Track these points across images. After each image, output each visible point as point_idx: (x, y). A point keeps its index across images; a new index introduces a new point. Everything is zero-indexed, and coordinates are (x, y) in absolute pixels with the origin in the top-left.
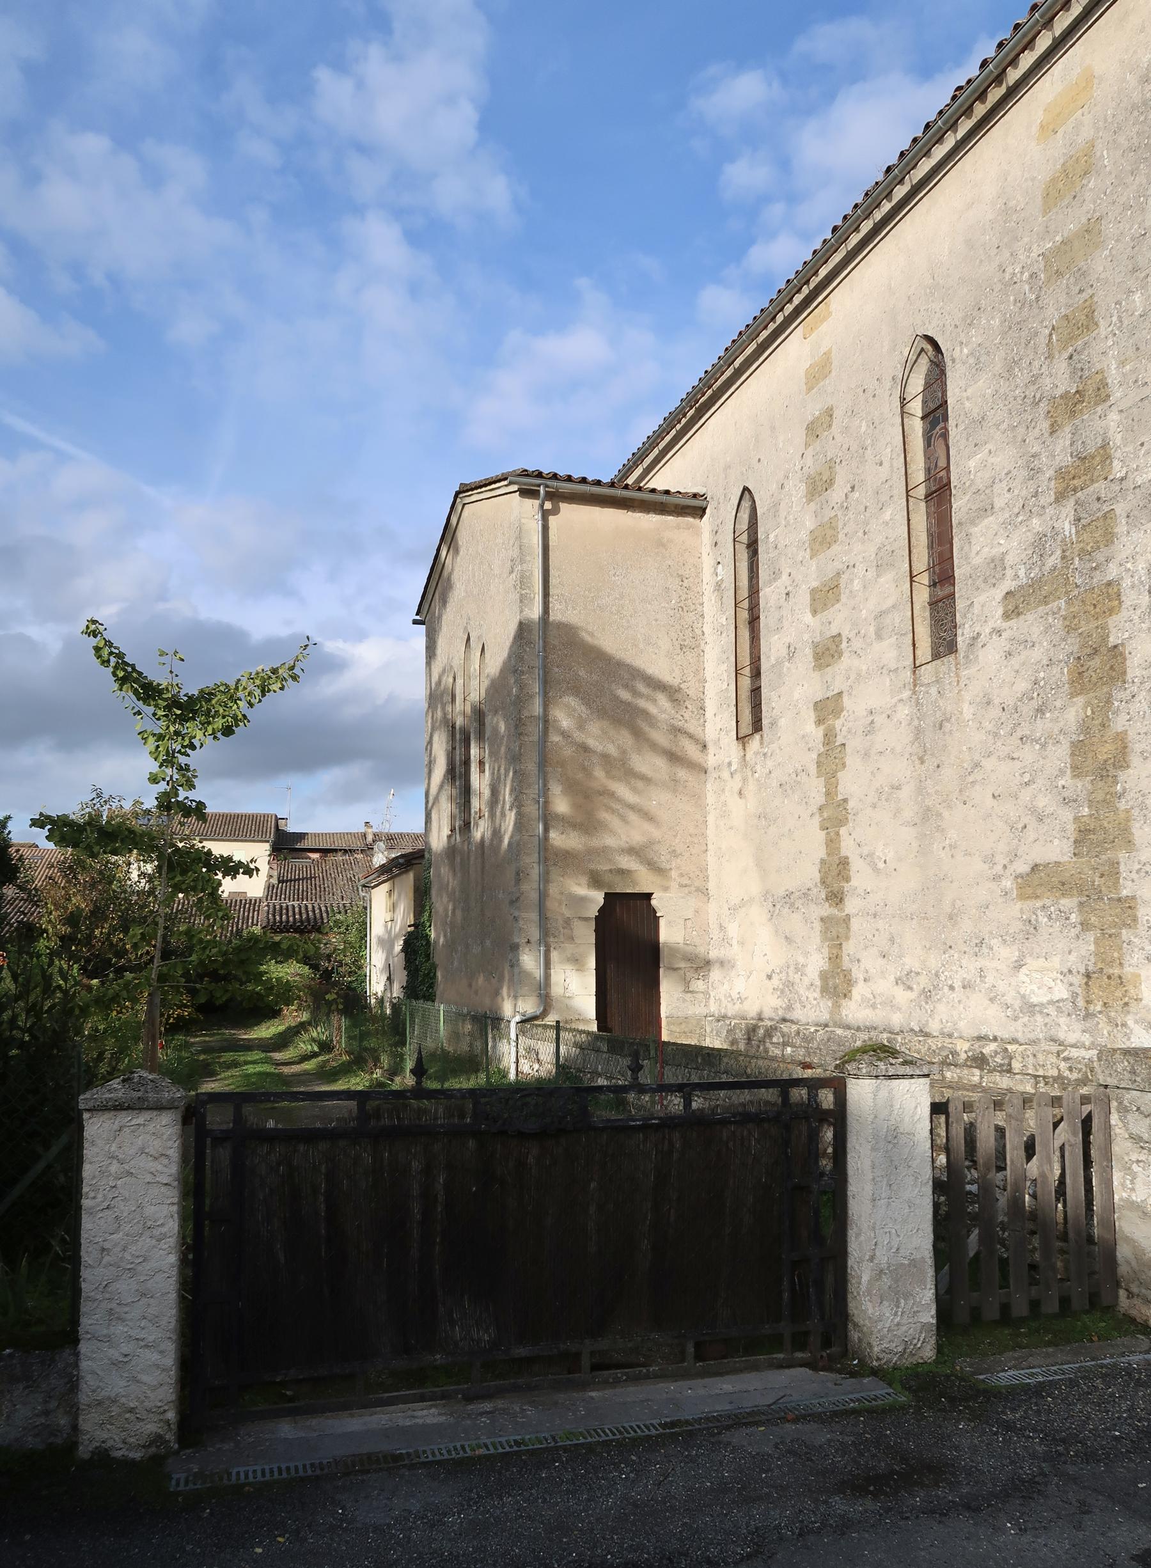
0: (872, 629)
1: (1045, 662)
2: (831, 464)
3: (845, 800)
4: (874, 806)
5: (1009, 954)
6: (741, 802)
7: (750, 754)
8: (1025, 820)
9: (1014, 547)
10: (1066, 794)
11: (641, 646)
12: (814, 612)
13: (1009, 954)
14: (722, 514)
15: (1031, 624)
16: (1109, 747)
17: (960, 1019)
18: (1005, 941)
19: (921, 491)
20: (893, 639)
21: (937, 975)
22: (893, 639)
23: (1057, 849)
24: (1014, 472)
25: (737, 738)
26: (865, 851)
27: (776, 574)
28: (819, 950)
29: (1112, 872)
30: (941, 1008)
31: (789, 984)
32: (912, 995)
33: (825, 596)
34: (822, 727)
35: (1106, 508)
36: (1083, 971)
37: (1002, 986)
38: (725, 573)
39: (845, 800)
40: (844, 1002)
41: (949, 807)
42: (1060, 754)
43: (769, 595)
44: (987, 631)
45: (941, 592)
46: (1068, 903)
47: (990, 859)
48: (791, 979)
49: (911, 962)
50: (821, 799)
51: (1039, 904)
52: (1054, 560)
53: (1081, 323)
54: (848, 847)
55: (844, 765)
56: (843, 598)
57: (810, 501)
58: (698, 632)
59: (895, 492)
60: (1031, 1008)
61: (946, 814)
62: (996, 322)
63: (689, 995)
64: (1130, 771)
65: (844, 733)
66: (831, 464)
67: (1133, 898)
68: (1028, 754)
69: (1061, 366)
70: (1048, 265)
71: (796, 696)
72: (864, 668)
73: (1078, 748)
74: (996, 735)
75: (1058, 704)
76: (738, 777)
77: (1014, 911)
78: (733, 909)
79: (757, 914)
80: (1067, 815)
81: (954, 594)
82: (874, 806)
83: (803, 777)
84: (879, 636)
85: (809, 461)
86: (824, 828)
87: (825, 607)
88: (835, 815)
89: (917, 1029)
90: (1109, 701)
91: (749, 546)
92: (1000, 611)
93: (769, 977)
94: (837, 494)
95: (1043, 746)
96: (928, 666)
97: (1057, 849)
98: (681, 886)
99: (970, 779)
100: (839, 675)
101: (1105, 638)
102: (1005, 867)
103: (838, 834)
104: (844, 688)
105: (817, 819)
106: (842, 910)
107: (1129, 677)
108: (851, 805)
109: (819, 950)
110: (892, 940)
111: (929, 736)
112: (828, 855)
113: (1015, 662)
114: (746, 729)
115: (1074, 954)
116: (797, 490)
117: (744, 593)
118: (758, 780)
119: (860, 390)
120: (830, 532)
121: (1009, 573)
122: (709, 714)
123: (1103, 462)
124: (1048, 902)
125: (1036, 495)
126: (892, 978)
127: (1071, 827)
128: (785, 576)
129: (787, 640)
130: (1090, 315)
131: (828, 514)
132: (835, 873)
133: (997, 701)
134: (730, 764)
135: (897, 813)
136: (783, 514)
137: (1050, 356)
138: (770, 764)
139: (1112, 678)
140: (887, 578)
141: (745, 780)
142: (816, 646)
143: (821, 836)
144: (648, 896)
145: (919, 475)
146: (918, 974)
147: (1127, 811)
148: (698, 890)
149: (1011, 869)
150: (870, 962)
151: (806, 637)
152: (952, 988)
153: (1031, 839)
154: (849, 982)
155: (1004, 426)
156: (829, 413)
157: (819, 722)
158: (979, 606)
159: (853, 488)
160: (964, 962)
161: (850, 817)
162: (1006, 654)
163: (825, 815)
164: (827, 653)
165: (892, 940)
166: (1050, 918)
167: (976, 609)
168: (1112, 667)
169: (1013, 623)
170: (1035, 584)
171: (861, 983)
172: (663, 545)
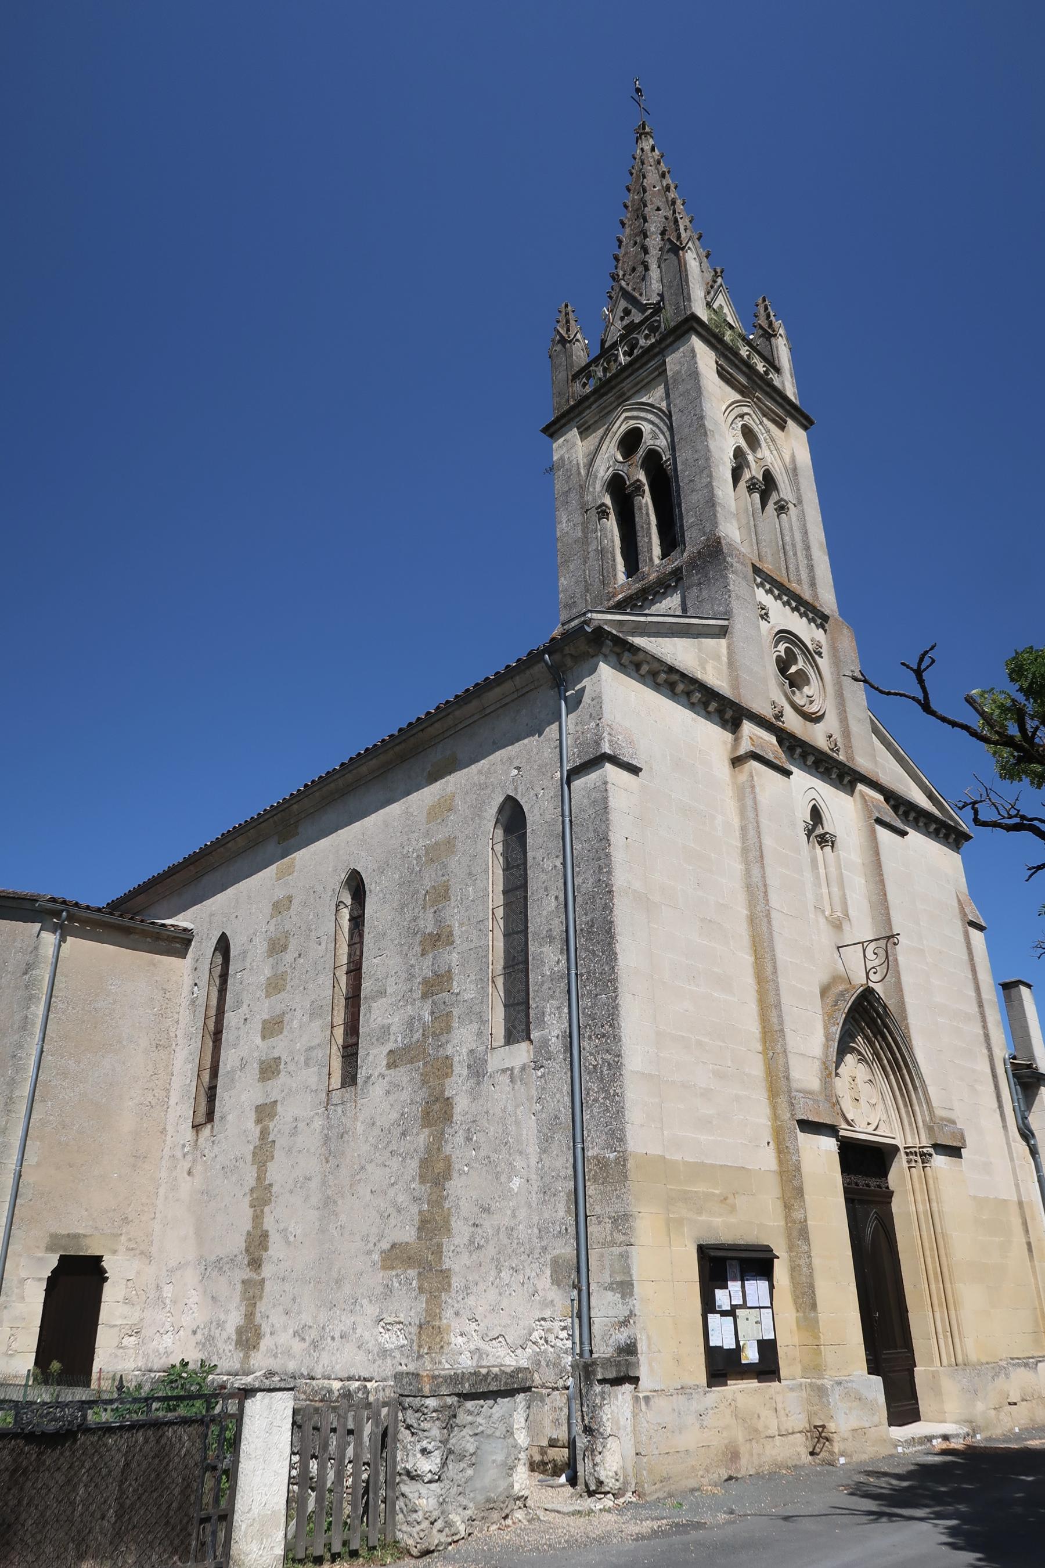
0: (302, 1059)
1: (409, 1101)
2: (287, 934)
3: (271, 1185)
4: (291, 1192)
5: (371, 1310)
6: (188, 1178)
7: (201, 1140)
8: (390, 1210)
9: (396, 1022)
10: (416, 1194)
11: (124, 1043)
12: (264, 1038)
13: (371, 1310)
14: (203, 948)
15: (402, 1075)
16: (441, 1164)
17: (337, 1363)
18: (371, 1301)
19: (345, 968)
20: (316, 1069)
21: (323, 1328)
22: (316, 1069)
23: (408, 1234)
24: (400, 973)
25: (193, 1127)
26: (282, 1226)
27: (239, 1004)
28: (237, 1308)
29: (438, 1251)
30: (325, 1355)
31: (210, 1339)
33: (272, 1027)
34: (260, 1126)
35: (448, 1009)
36: (418, 1323)
37: (367, 1335)
38: (201, 993)
39: (271, 1185)
40: (252, 1354)
41: (343, 1196)
42: (414, 1165)
43: (231, 1018)
44: (377, 1074)
45: (351, 1041)
46: (412, 1273)
47: (366, 1239)
48: (212, 1333)
49: (306, 1318)
50: (252, 1183)
51: (394, 1273)
52: (417, 1036)
53: (441, 895)
54: (269, 1223)
55: (273, 1157)
56: (285, 1033)
57: (269, 956)
58: (172, 1035)
59: (327, 966)
60: (384, 1353)
61: (340, 1202)
62: (396, 876)
63: (121, 1350)
64: (452, 1182)
65: (275, 1132)
66: (287, 934)
67: (450, 1270)
68: (395, 1163)
69: (429, 915)
70: (427, 853)
71: (243, 1098)
72: (294, 1085)
73: (424, 1163)
74: (376, 1147)
75: (415, 1131)
76: (189, 1157)
77: (376, 1279)
78: (171, 1271)
79: (191, 1276)
80: (415, 1210)
81: (357, 1044)
82: (291, 1192)
83: (241, 1164)
84: (307, 1064)
85: (272, 928)
86: (252, 1206)
87: (272, 1035)
88: (261, 1196)
89: (305, 1373)
90: (443, 1134)
91: (220, 976)
92: (385, 1063)
93: (194, 1333)
94: (289, 956)
95: (404, 1159)
96: (337, 1092)
97: (408, 1234)
98: (129, 1249)
99: (358, 1177)
100: (275, 1089)
101: (443, 1092)
102: (375, 1244)
103: (262, 1211)
104: (279, 1098)
105: (248, 1199)
106: (259, 1274)
107: (454, 1120)
108: (274, 1189)
109: (237, 1308)
110: (294, 1300)
111: (334, 1141)
112: (253, 1228)
113: (391, 1098)
114: (201, 1118)
115: (413, 1311)
116: (261, 947)
117: (213, 1012)
118: (205, 1162)
119: (311, 891)
120: (281, 982)
121: (392, 1037)
122: (172, 1102)
123: (448, 981)
124: (399, 1271)
125: (411, 991)
126: (291, 1331)
127: (417, 1218)
128: (245, 1006)
129: (242, 1054)
130: (447, 891)
131: (282, 969)
132: (257, 1243)
133: (378, 1124)
134: (184, 1146)
135: (307, 1198)
136: (249, 960)
137: (424, 908)
138: (216, 1149)
139: (445, 1119)
140: (316, 1025)
141: (194, 1161)
142: (262, 1063)
143: (250, 1212)
144: (99, 1258)
145: (344, 959)
146: (310, 1327)
147: (449, 1209)
148: (142, 1253)
149: (379, 1245)
150: (276, 1318)
151: (256, 1054)
152: (333, 1338)
153: (392, 1225)
154: (259, 1336)
155: (396, 942)
156: (290, 899)
157: (258, 1121)
158: (373, 1058)
159: (300, 955)
160: (343, 1318)
161: (273, 1198)
163: (255, 1196)
164: (269, 1069)
165: (294, 1300)
166: (400, 1284)
167: (371, 1058)
168: (445, 1112)
169: (391, 1072)
170: (407, 1049)
171: (268, 1335)
172: (154, 965)
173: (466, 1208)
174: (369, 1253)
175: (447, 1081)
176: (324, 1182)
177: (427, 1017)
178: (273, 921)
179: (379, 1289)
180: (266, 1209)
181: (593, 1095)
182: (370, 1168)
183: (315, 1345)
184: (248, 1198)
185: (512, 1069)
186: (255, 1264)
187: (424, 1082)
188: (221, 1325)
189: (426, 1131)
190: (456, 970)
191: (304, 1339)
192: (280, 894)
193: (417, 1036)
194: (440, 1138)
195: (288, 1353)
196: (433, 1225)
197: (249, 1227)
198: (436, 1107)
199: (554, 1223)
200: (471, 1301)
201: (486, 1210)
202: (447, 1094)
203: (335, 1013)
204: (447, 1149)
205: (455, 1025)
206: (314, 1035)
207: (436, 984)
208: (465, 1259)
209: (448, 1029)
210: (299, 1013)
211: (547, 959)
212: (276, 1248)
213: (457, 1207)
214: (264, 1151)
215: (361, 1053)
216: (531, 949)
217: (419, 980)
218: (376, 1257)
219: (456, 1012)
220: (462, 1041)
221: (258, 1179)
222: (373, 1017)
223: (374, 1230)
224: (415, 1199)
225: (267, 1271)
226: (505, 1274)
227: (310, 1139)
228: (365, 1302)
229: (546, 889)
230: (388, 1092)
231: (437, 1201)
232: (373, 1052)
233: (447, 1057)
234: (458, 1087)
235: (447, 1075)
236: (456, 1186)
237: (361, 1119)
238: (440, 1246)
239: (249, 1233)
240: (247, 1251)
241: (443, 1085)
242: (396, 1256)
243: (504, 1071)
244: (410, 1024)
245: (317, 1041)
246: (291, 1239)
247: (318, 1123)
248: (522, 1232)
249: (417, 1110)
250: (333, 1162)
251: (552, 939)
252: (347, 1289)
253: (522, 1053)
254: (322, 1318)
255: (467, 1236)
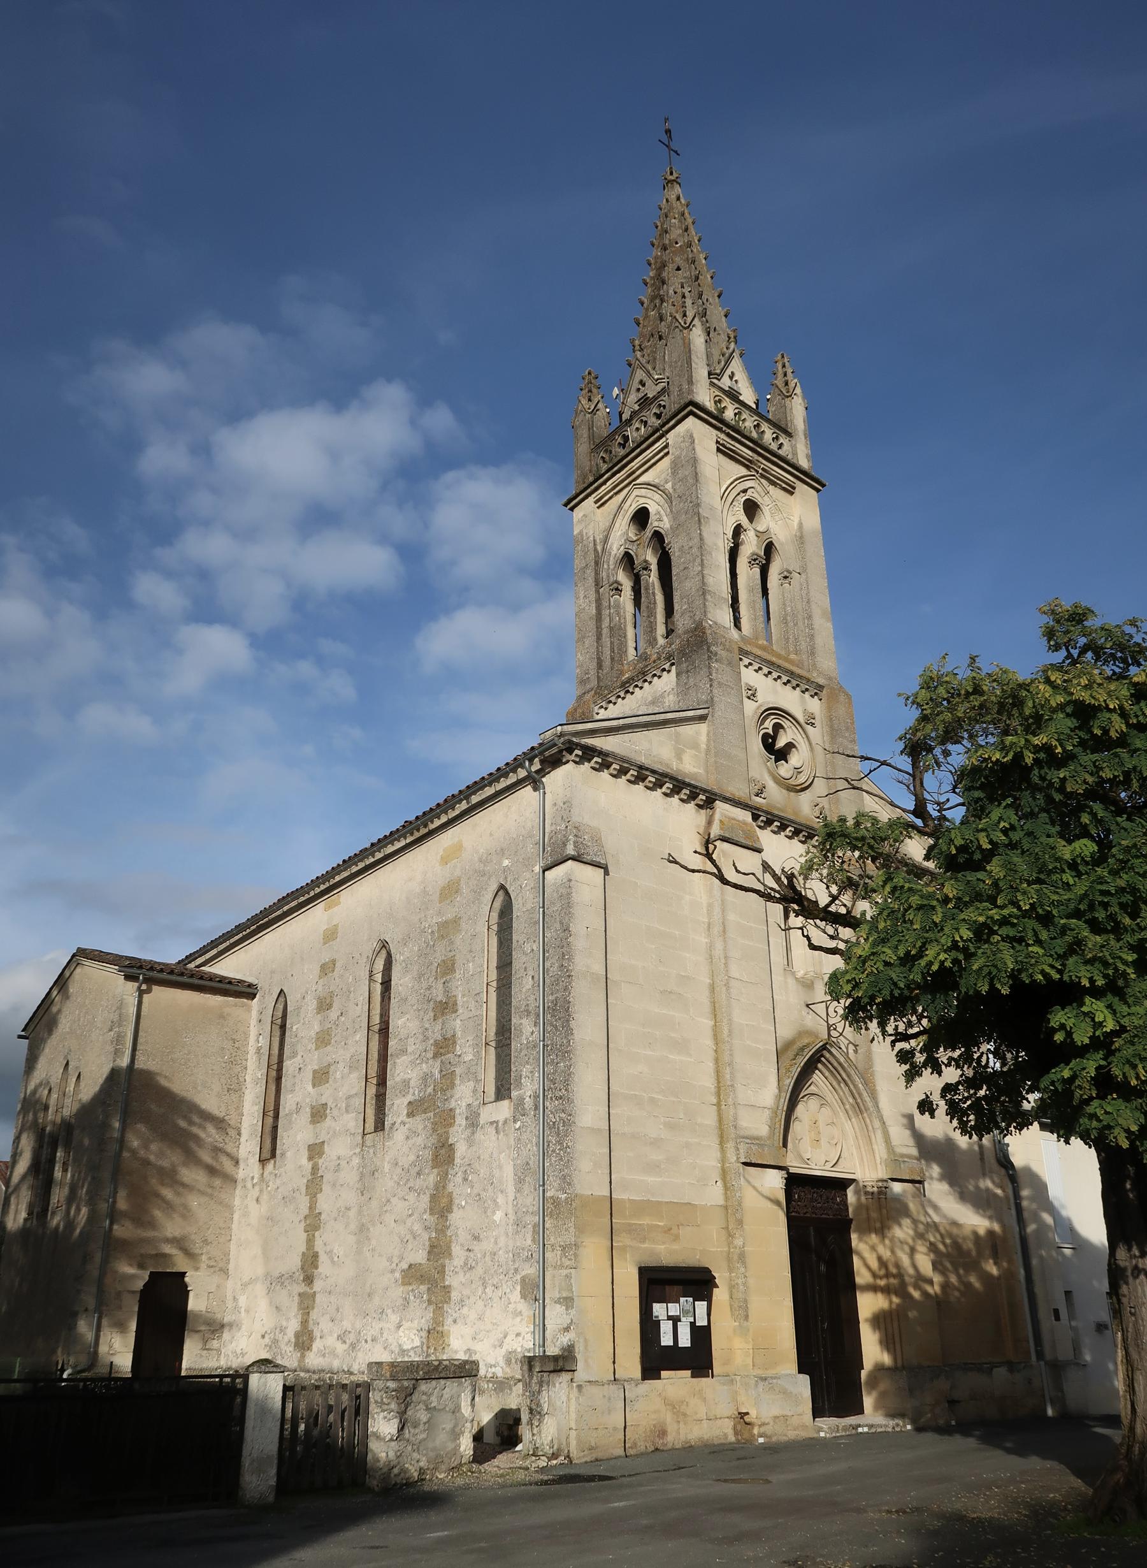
15: (418, 1123)
23: (419, 1256)
29: (442, 1271)
32: (345, 1347)
42: (426, 1199)
46: (423, 1288)
47: (390, 1259)
49: (346, 1324)
68: (412, 1197)
73: (434, 1198)
77: (398, 1292)
97: (419, 1256)
113: (410, 1142)
124: (414, 1287)
127: (427, 1243)
154: (311, 1339)
158: (397, 1106)
162: (406, 1139)
170: (422, 1101)
173: (463, 1236)
174: (393, 1271)
175: (452, 1130)
176: (360, 1212)
177: (437, 1075)
178: (321, 982)
179: (400, 1301)
180: (317, 1234)
181: (552, 1147)
182: (394, 1201)
183: (353, 1346)
184: (303, 1224)
185: (497, 1122)
186: (309, 1280)
187: (434, 1130)
188: (283, 1330)
189: (435, 1171)
190: (459, 1034)
191: (345, 1342)
192: (326, 957)
193: (430, 1090)
194: (444, 1178)
195: (333, 1353)
196: (439, 1250)
197: (303, 1248)
198: (443, 1151)
199: (523, 1249)
200: (465, 1310)
201: (476, 1238)
202: (450, 1141)
203: (369, 1067)
204: (450, 1187)
205: (457, 1082)
206: (350, 1084)
207: (444, 1046)
208: (461, 1277)
209: (452, 1085)
210: (341, 1066)
211: (526, 1030)
212: (324, 1267)
213: (457, 1235)
214: (314, 1185)
215: (388, 1103)
216: (514, 1021)
217: (432, 1041)
218: (398, 1275)
219: (458, 1071)
220: (463, 1096)
221: (310, 1208)
222: (398, 1072)
223: (396, 1253)
224: (426, 1228)
225: (318, 1285)
226: (489, 1290)
227: (349, 1176)
228: (389, 1311)
229: (525, 969)
230: (408, 1138)
231: (442, 1228)
232: (397, 1102)
233: (451, 1110)
234: (458, 1134)
235: (451, 1125)
236: (455, 1217)
237: (387, 1159)
238: (444, 1266)
239: (303, 1254)
240: (302, 1269)
241: (447, 1133)
242: (412, 1275)
243: (492, 1123)
244: (425, 1078)
245: (353, 1092)
246: (336, 1259)
247: (356, 1161)
248: (502, 1256)
249: (428, 1154)
250: (367, 1196)
251: (528, 1013)
252: (376, 1300)
253: (504, 1109)
254: (358, 1326)
255: (463, 1259)
